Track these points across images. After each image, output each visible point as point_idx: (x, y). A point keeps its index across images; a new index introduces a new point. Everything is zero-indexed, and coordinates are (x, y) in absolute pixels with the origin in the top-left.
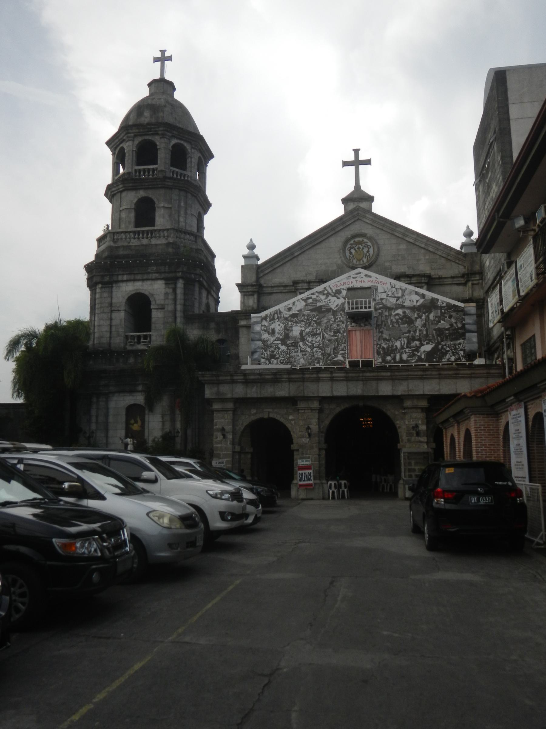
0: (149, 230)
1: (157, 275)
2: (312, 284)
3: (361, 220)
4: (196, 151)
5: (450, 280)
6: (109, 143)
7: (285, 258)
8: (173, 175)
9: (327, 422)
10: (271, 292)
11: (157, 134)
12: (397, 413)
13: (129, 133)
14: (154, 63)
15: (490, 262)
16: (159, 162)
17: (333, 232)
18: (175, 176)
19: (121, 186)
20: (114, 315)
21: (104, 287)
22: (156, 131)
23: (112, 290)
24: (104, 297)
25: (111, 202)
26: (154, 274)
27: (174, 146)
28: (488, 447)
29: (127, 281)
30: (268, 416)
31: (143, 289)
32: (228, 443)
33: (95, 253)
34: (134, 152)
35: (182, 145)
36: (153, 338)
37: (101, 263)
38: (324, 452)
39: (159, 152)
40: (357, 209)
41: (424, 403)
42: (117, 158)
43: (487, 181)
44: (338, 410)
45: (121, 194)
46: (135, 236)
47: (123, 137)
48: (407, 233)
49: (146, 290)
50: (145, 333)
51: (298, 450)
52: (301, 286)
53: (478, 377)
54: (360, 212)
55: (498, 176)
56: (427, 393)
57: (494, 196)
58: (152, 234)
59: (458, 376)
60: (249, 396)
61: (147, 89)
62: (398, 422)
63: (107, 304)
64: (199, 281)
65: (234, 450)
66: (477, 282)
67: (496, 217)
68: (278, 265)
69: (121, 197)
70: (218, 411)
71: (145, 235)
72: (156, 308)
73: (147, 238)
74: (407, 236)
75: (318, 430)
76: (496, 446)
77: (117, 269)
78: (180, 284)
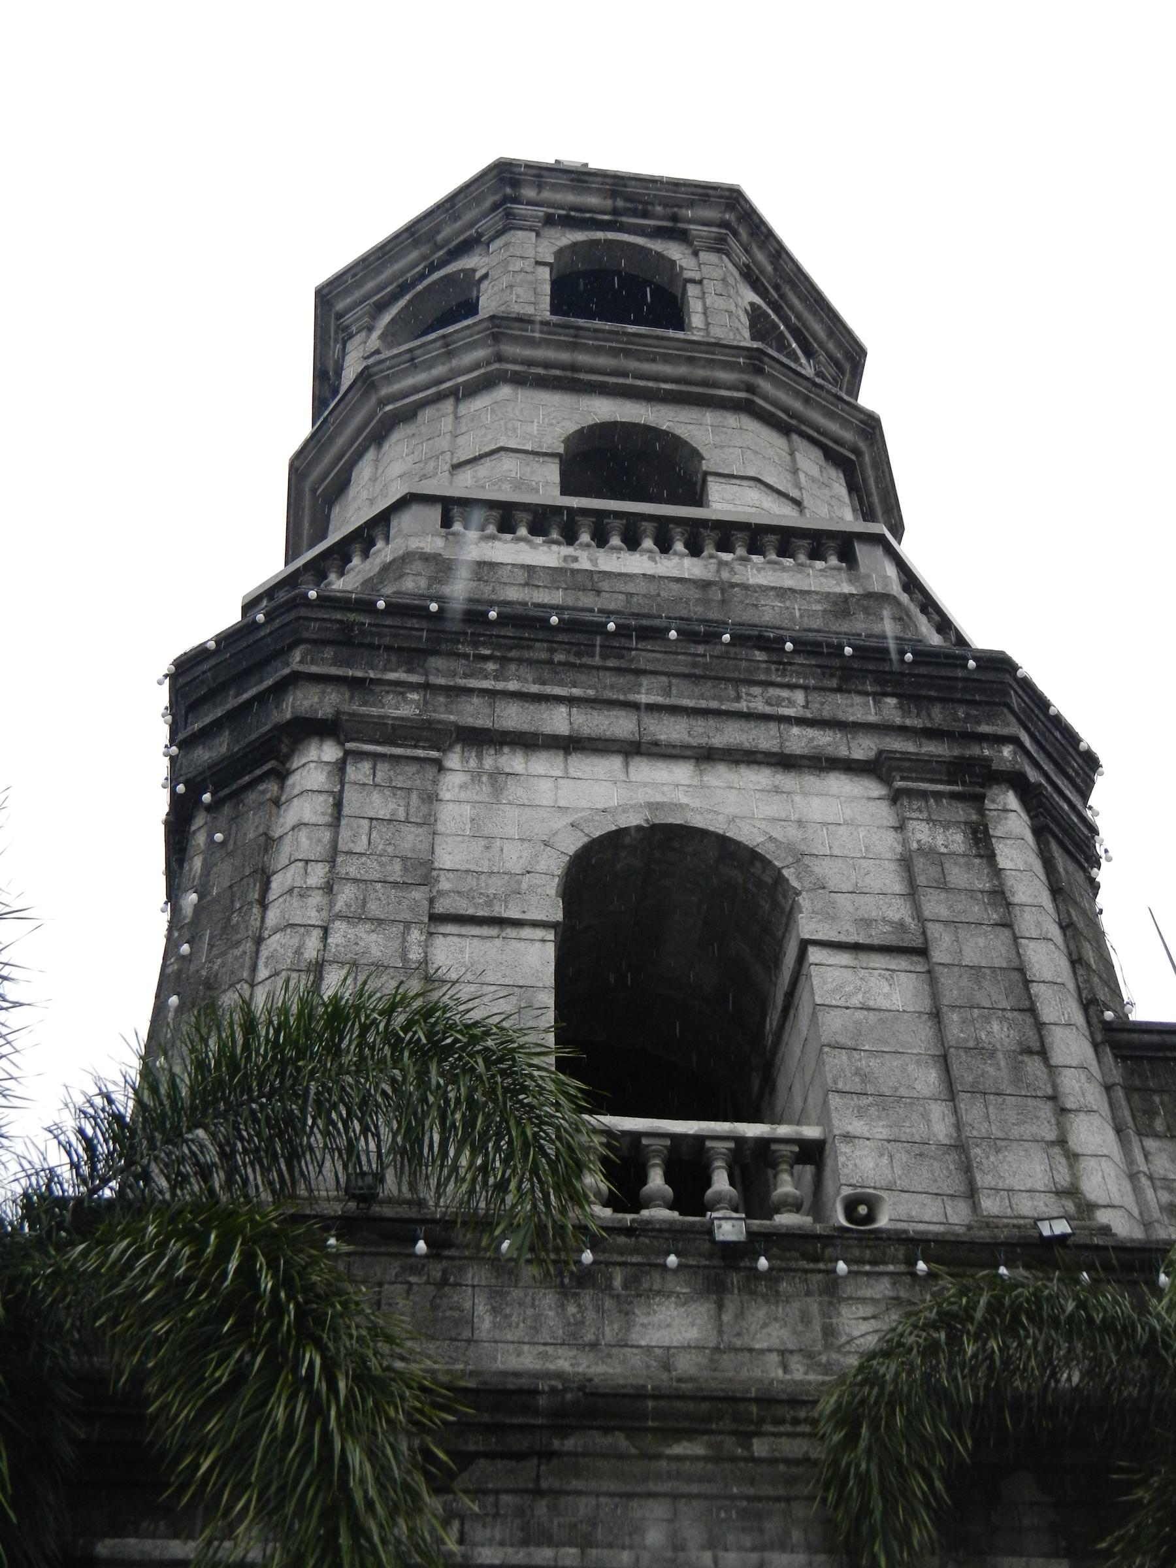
1: (824, 740)
11: (680, 235)
13: (516, 200)
16: (697, 320)
21: (375, 757)
22: (675, 218)
23: (435, 782)
24: (371, 819)
26: (795, 730)
31: (717, 813)
45: (456, 407)
49: (732, 820)
63: (397, 866)
72: (843, 938)
77: (491, 666)
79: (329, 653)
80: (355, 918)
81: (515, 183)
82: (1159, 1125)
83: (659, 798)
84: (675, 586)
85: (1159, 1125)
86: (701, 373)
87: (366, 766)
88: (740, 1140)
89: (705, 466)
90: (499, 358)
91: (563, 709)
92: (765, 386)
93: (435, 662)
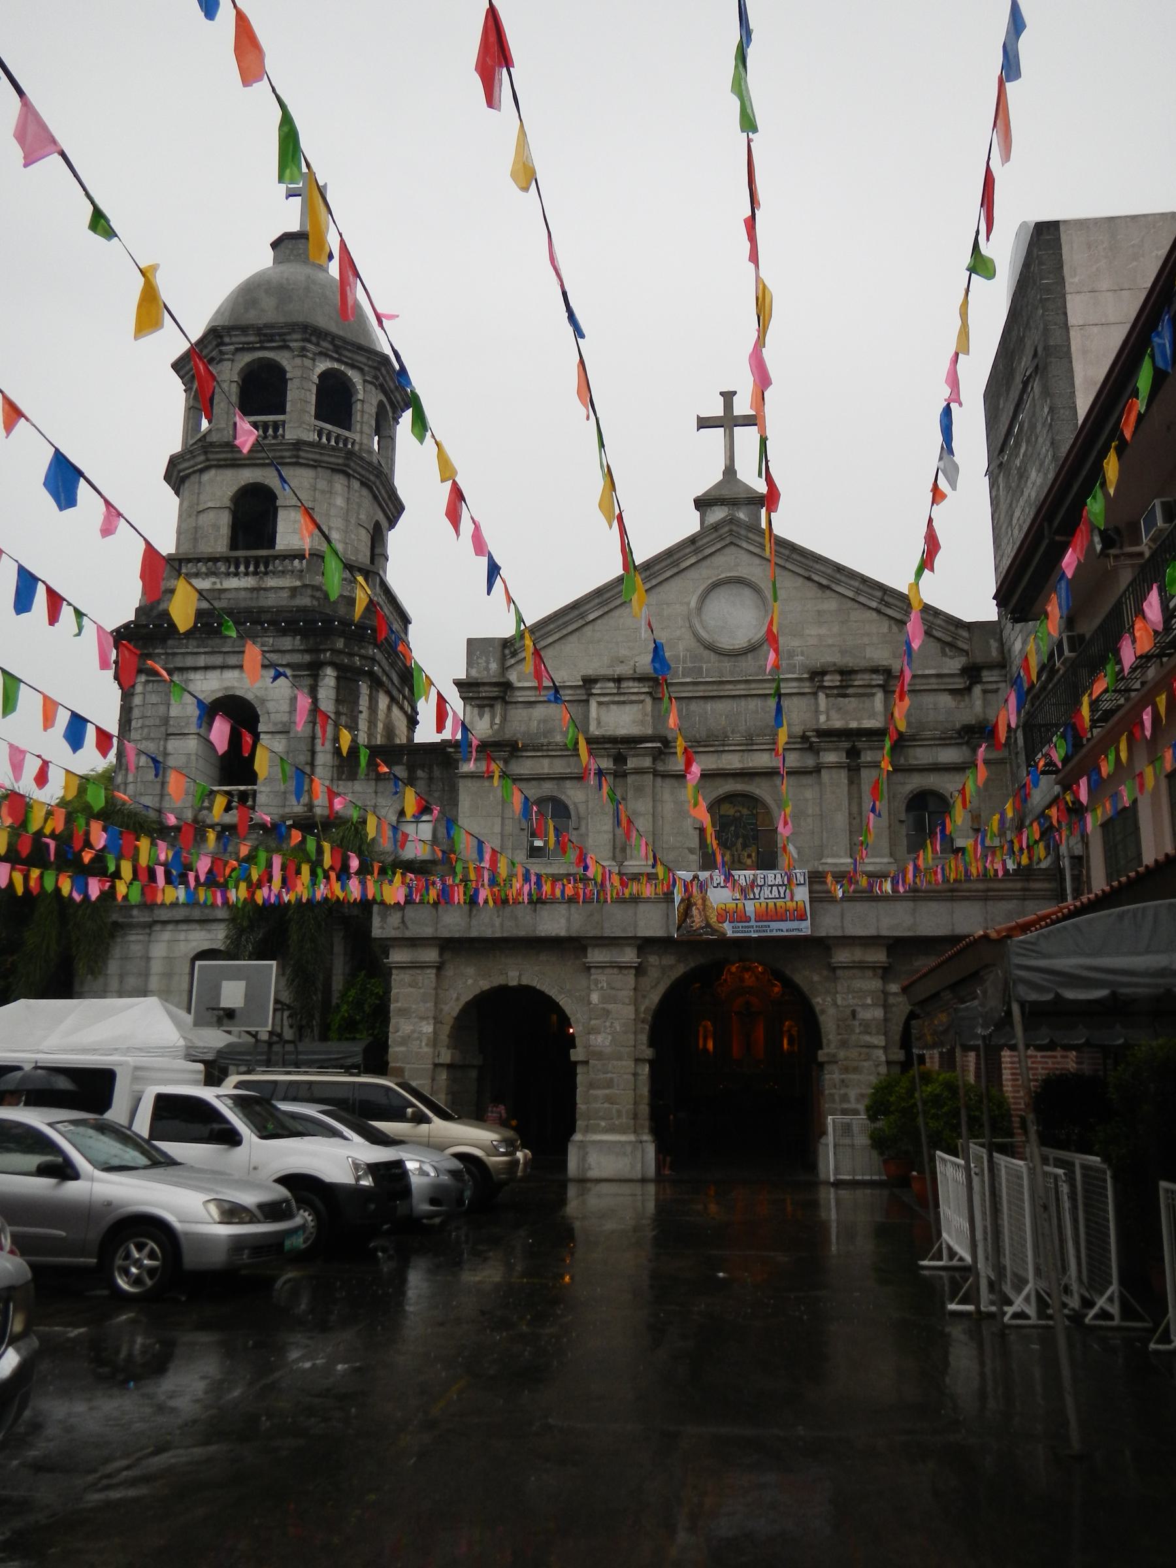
0: (262, 557)
2: (624, 684)
3: (738, 546)
4: (374, 388)
5: (933, 680)
6: (178, 366)
7: (566, 624)
8: (320, 438)
9: (655, 998)
10: (533, 699)
11: (288, 348)
12: (816, 978)
13: (223, 344)
14: (287, 198)
15: (1024, 643)
16: (288, 409)
17: (675, 570)
18: (324, 440)
19: (202, 458)
20: (173, 745)
22: (284, 341)
25: (177, 493)
27: (323, 376)
28: (1040, 1062)
29: (206, 668)
30: (519, 980)
32: (423, 1044)
33: (138, 606)
34: (235, 384)
35: (345, 374)
36: (261, 799)
37: (147, 626)
38: (646, 1069)
39: (290, 385)
40: (731, 521)
41: (879, 956)
42: (195, 398)
43: (1018, 462)
44: (681, 970)
45: (200, 478)
46: (229, 568)
47: (212, 351)
48: (838, 576)
50: (242, 788)
51: (586, 1063)
52: (601, 688)
53: (1002, 898)
54: (734, 528)
55: (1044, 450)
56: (885, 933)
57: (1033, 495)
58: (266, 567)
59: (955, 894)
60: (474, 934)
61: (270, 253)
62: (819, 1000)
64: (371, 674)
65: (437, 1062)
66: (994, 686)
67: (1046, 532)
68: (550, 640)
69: (200, 482)
70: (403, 968)
71: (251, 569)
73: (256, 573)
74: (838, 582)
75: (633, 1017)
76: (1059, 1059)
77: (185, 641)
78: (329, 678)
79: (140, 643)
80: (146, 739)
81: (221, 337)
82: (344, 777)
83: (229, 685)
84: (243, 593)
85: (344, 777)
86: (278, 454)
87: (151, 685)
88: (241, 792)
89: (279, 503)
90: (208, 460)
91: (203, 656)
92: (302, 454)
93: (170, 642)
